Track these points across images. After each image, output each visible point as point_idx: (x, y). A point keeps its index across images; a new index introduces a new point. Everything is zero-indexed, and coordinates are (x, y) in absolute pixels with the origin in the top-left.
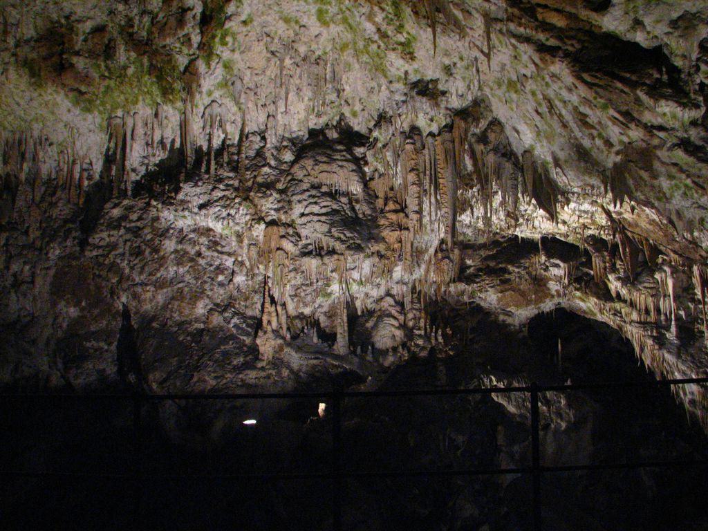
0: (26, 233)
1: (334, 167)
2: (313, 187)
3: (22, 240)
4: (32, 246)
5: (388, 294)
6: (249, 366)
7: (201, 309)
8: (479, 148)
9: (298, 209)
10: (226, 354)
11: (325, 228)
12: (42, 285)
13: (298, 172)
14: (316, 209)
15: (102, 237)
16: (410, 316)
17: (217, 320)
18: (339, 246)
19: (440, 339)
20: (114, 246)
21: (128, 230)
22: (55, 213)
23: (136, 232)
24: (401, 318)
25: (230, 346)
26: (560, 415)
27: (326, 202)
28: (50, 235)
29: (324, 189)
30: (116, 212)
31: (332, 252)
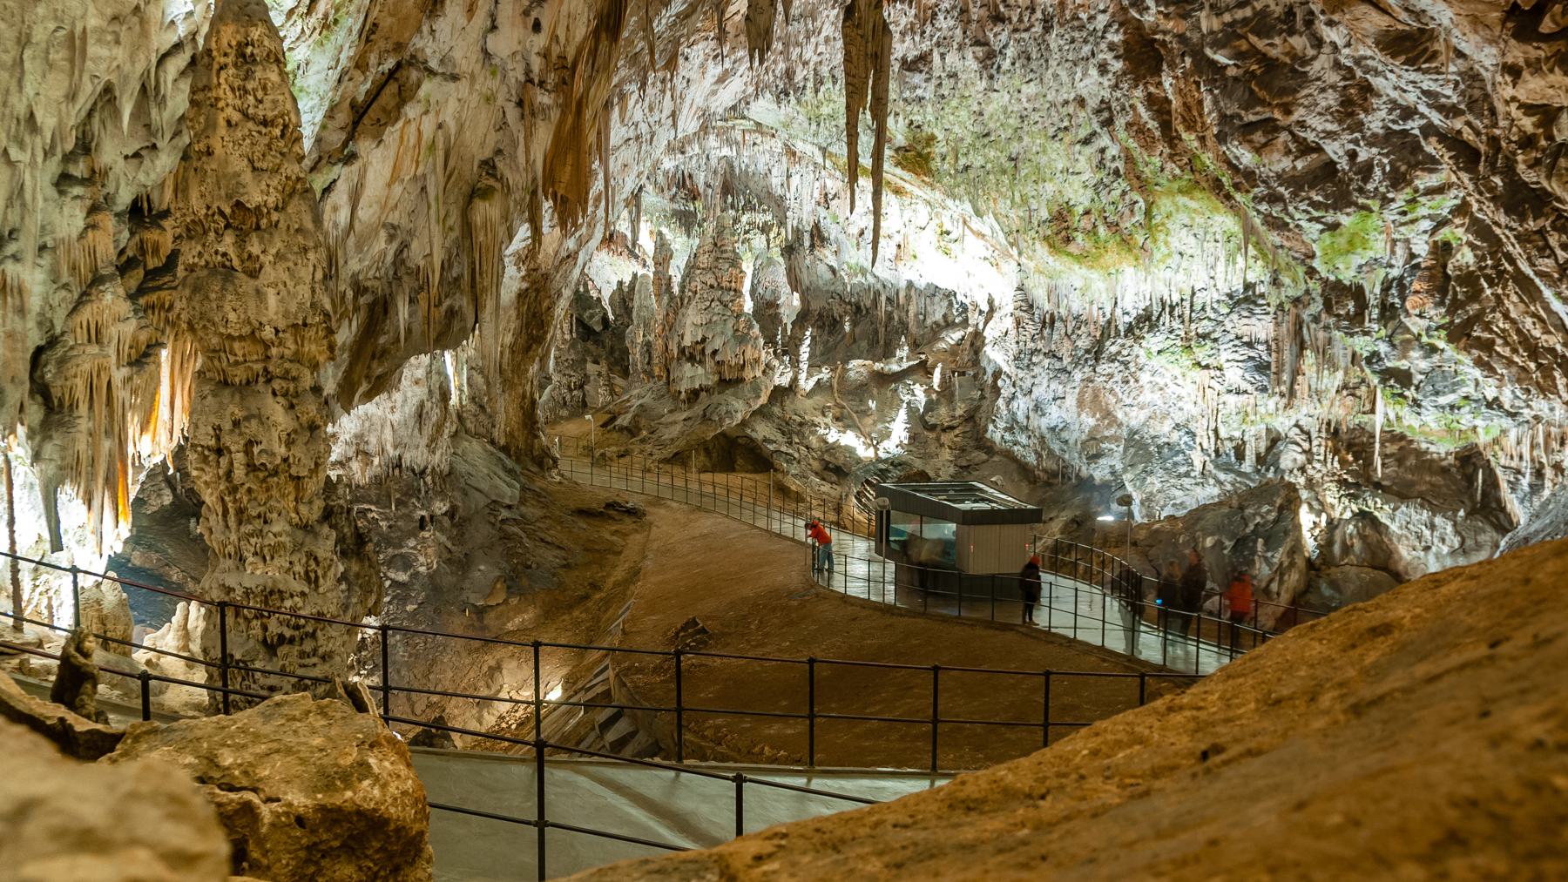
0: (1060, 359)
1: (1253, 320)
2: (1237, 338)
3: (1058, 365)
4: (1064, 370)
5: (1297, 425)
6: (1187, 475)
7: (1167, 427)
8: (1313, 326)
9: (1224, 356)
10: (1175, 464)
11: (1241, 372)
12: (1071, 400)
13: (1228, 326)
14: (1237, 357)
15: (1104, 368)
16: (1315, 443)
17: (1175, 436)
18: (1250, 388)
19: (1336, 464)
20: (1111, 376)
21: (1122, 363)
22: (1079, 343)
23: (1126, 364)
24: (1306, 446)
25: (1180, 458)
26: (1443, 540)
27: (1245, 351)
28: (1076, 363)
29: (1246, 339)
30: (1114, 349)
31: (1246, 392)
